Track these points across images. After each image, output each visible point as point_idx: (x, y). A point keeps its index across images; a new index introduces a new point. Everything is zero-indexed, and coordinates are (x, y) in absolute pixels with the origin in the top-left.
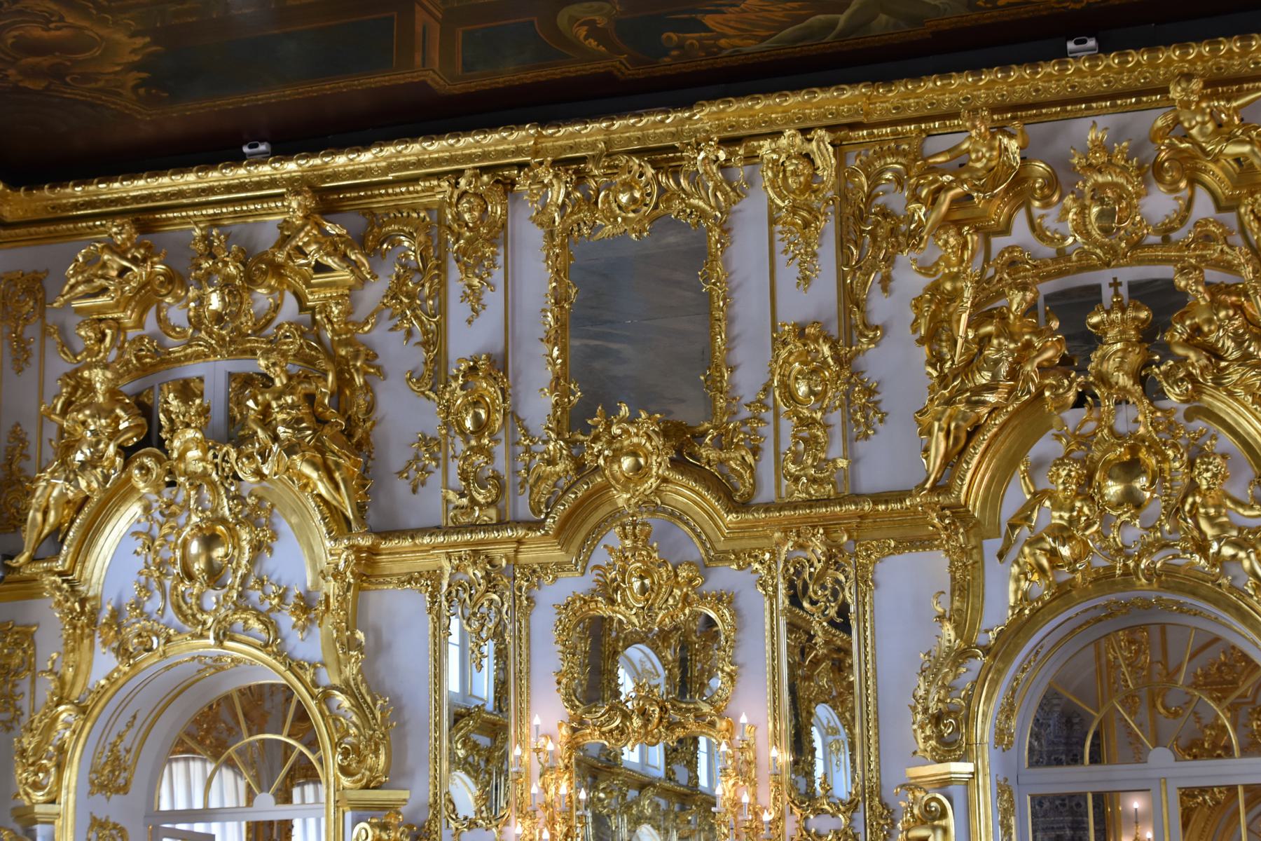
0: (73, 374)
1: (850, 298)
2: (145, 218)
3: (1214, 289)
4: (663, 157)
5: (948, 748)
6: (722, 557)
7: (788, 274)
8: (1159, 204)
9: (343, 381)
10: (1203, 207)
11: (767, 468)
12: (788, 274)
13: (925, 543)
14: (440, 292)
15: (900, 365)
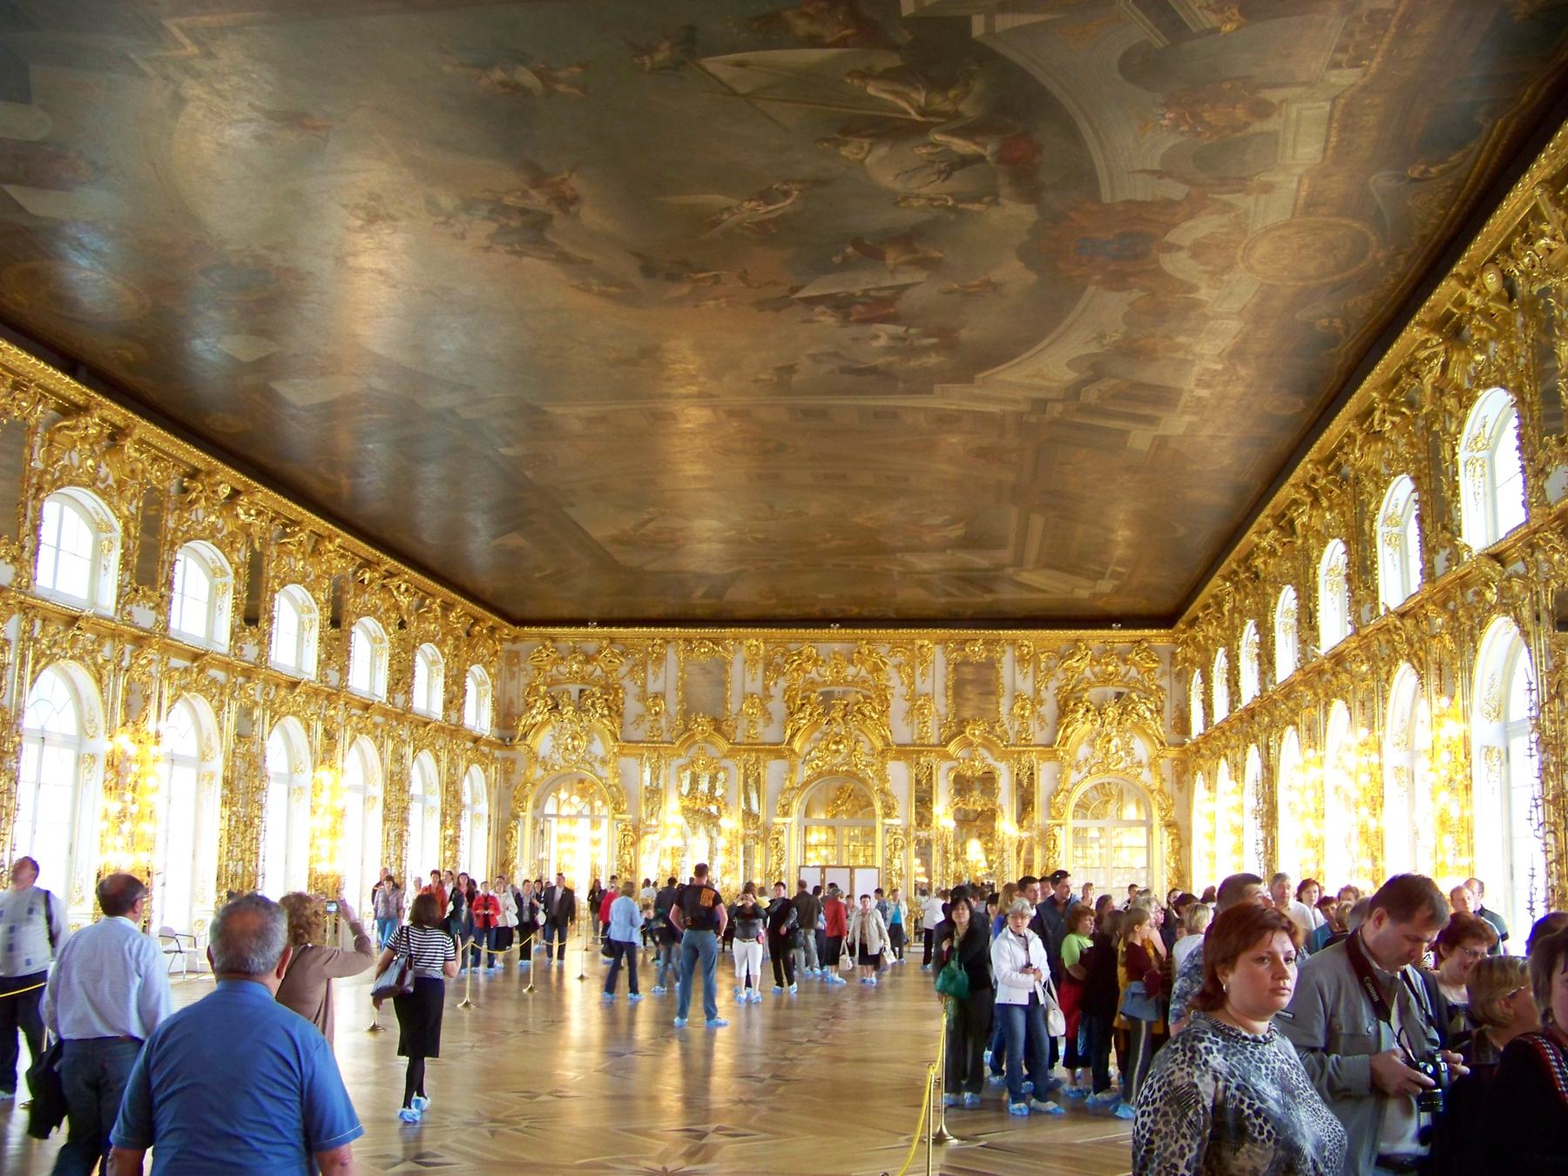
0: (529, 685)
1: (766, 688)
2: (553, 640)
3: (865, 697)
4: (716, 642)
5: (786, 814)
6: (725, 757)
7: (748, 678)
8: (851, 670)
9: (617, 694)
10: (863, 672)
11: (738, 732)
12: (748, 678)
13: (783, 758)
14: (645, 670)
15: (777, 706)
